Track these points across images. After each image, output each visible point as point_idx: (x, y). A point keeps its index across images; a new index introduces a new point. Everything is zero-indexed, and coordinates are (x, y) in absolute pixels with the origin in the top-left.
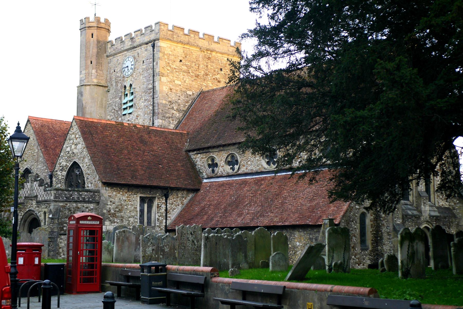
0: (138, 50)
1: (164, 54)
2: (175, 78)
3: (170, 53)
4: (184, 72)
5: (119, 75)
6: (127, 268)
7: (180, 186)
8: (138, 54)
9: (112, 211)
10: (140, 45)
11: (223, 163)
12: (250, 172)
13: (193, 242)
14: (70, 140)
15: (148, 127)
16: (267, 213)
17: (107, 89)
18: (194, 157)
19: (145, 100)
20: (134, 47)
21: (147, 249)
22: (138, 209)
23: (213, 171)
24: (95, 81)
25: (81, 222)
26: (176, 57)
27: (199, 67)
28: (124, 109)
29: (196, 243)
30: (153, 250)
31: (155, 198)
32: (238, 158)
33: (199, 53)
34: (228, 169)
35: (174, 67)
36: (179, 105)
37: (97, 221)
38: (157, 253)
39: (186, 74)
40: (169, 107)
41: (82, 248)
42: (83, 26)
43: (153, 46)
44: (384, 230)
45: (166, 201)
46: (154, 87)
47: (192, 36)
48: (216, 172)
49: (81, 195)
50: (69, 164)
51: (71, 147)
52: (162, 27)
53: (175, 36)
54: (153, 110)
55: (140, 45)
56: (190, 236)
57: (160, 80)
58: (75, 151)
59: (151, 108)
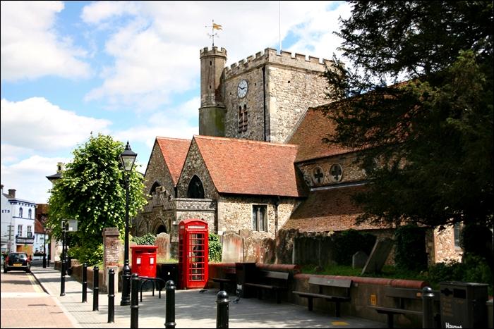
0: (251, 74)
9: (228, 218)
11: (327, 173)
23: (319, 181)
28: (240, 128)
30: (254, 251)
43: (264, 70)
46: (265, 106)
48: (322, 181)
49: (200, 205)
51: (192, 162)
54: (265, 127)
58: (195, 166)
59: (263, 125)
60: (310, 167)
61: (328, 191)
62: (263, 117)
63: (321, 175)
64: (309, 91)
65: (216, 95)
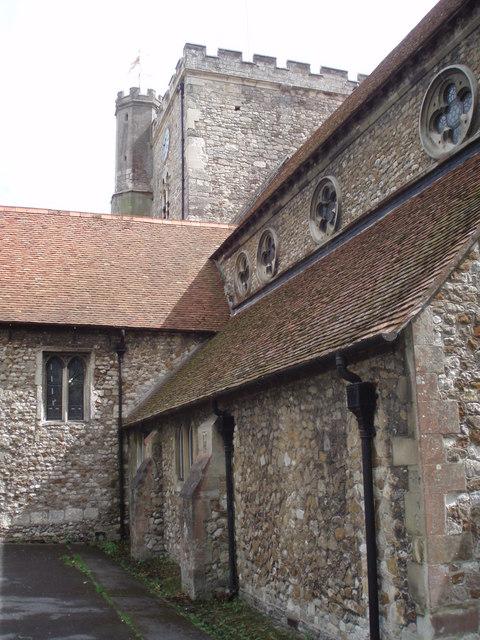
24: (130, 186)
27: (278, 118)
31: (87, 355)
65: (134, 171)
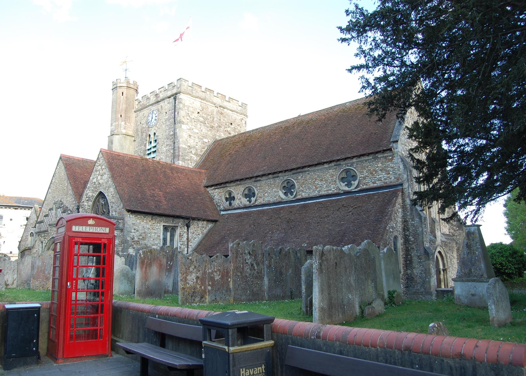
0: (162, 104)
1: (184, 105)
2: (193, 127)
3: (190, 105)
4: (201, 122)
5: (144, 126)
6: (160, 314)
7: (200, 217)
8: (162, 107)
9: (136, 239)
10: (163, 100)
11: (240, 196)
12: (267, 202)
13: (252, 265)
14: (96, 171)
15: (170, 164)
16: (292, 239)
17: (133, 139)
18: (212, 192)
19: (167, 145)
20: (158, 102)
21: (189, 277)
22: (162, 237)
23: (230, 204)
25: (75, 228)
26: (195, 109)
29: (256, 268)
30: (197, 278)
32: (255, 190)
33: (214, 108)
34: (245, 201)
35: (193, 117)
36: (197, 150)
37: (106, 226)
38: (203, 283)
39: (202, 124)
40: (188, 151)
41: (74, 276)
42: (115, 86)
43: (175, 99)
44: (414, 253)
45: (188, 230)
46: (175, 134)
47: (208, 93)
48: (233, 205)
50: (95, 195)
51: (97, 178)
52: (183, 83)
53: (194, 92)
55: (163, 100)
56: (249, 257)
57: (181, 127)
58: (101, 181)
59: (172, 151)
60: (221, 190)
61: (241, 213)
62: (172, 143)
63: (233, 198)
64: (216, 124)
